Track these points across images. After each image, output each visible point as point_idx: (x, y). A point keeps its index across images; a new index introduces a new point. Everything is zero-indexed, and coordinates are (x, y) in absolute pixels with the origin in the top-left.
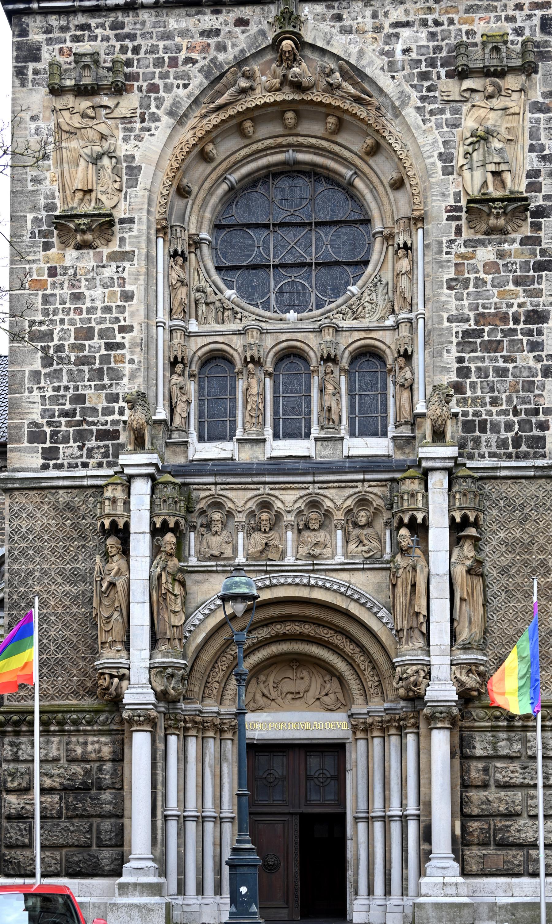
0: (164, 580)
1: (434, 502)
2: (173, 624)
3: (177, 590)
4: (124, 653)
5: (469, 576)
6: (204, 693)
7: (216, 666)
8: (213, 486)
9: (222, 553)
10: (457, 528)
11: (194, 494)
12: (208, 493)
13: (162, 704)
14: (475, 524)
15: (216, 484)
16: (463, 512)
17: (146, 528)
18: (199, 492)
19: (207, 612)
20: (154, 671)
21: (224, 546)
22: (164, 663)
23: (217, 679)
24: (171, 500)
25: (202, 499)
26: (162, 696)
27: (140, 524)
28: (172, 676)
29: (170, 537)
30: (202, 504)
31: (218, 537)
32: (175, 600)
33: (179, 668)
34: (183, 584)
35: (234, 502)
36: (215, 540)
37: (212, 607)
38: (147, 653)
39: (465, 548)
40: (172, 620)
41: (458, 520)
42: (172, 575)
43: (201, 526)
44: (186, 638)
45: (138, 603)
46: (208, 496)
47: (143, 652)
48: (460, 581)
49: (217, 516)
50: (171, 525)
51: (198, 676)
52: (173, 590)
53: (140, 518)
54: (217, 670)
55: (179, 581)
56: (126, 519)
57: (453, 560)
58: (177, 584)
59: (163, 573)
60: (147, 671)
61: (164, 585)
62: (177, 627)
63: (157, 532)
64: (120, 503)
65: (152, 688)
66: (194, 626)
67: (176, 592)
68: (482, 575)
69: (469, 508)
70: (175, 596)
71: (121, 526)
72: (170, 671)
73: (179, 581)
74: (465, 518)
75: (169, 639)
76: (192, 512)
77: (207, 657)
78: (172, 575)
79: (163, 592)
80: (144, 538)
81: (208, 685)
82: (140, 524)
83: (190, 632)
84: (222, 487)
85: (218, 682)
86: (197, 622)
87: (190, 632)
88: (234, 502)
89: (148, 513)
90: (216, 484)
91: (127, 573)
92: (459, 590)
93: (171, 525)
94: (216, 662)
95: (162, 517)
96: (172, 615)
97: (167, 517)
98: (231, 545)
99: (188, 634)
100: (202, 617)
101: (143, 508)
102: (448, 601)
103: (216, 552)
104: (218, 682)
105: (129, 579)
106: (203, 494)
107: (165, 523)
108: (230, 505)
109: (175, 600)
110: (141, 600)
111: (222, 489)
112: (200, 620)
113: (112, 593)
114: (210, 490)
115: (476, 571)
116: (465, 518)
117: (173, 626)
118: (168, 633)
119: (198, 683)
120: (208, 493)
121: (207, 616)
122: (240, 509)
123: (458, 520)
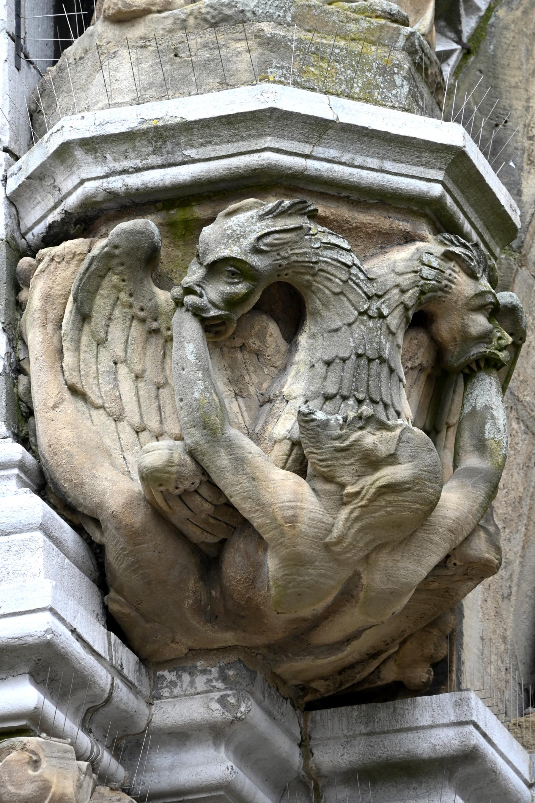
13: (191, 701)
22: (162, 138)
65: (43, 484)
72: (237, 230)
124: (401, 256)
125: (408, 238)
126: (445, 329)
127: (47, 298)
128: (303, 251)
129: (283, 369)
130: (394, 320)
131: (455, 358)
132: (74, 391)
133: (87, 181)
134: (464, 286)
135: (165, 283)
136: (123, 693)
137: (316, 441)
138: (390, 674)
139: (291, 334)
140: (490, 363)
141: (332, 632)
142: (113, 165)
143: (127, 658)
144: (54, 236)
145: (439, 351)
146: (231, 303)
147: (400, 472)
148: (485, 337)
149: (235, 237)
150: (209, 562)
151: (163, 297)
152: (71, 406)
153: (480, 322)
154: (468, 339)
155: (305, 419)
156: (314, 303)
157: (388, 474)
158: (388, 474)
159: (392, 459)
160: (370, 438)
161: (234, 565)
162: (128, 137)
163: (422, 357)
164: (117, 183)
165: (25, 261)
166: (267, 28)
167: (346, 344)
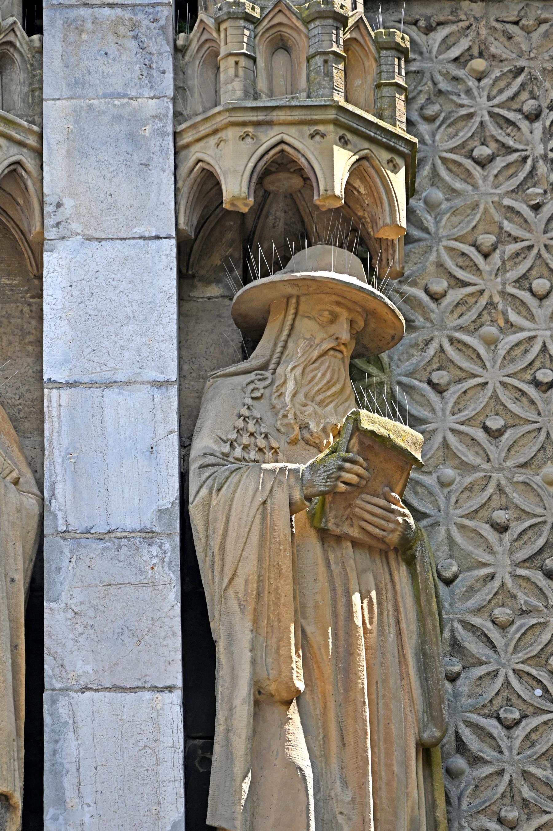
1: (77, 86)
5: (313, 546)
10: (227, 246)
14: (355, 231)
16: (269, 138)
39: (289, 375)
41: (235, 188)
48: (248, 569)
57: (203, 442)
68: (405, 550)
69: (310, 118)
74: (279, 171)
92: (244, 637)
102: (172, 706)
115: (359, 512)
116: (279, 171)
123: (235, 188)
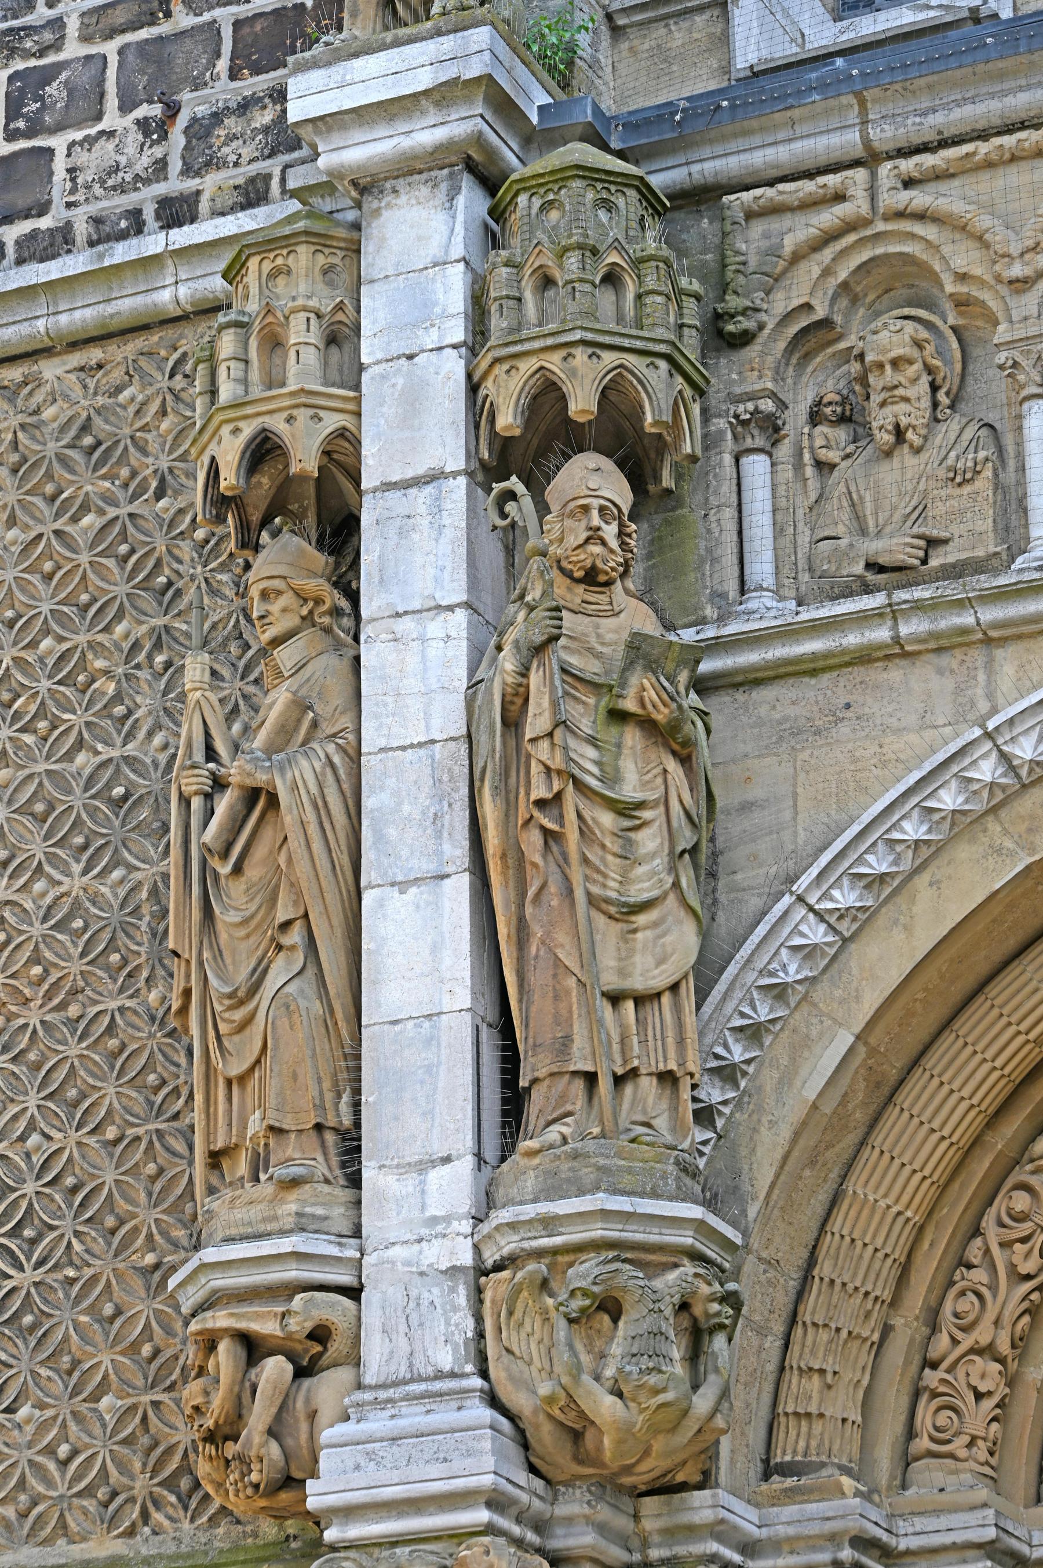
0: (538, 720)
2: (611, 981)
3: (638, 770)
4: (327, 1201)
6: (911, 1433)
7: (974, 1252)
8: (860, 175)
9: (932, 543)
11: (751, 242)
12: (828, 217)
13: (573, 1504)
15: (869, 159)
17: (447, 446)
18: (776, 224)
19: (845, 897)
20: (496, 1286)
21: (946, 502)
22: (549, 1223)
23: (982, 1335)
24: (573, 260)
25: (796, 258)
26: (550, 1446)
27: (414, 430)
28: (611, 1307)
29: (591, 479)
30: (805, 288)
31: (911, 461)
32: (624, 835)
33: (651, 1258)
34: (670, 737)
35: (981, 240)
36: (896, 481)
37: (878, 864)
38: (454, 1186)
40: (608, 959)
42: (595, 687)
43: (815, 418)
44: (727, 1073)
45: (403, 886)
46: (829, 237)
47: (437, 1176)
49: (890, 337)
50: (582, 403)
51: (848, 1314)
52: (612, 778)
53: (413, 401)
54: (979, 1276)
55: (647, 724)
56: (332, 422)
58: (632, 737)
59: (535, 679)
60: (462, 1297)
61: (542, 751)
62: (640, 1000)
63: (514, 459)
64: (302, 335)
65: (493, 1401)
66: (779, 992)
67: (630, 790)
70: (625, 809)
71: (305, 459)
72: (585, 1272)
73: (647, 724)
75: (591, 1078)
76: (745, 339)
77: (889, 1188)
78: (595, 687)
79: (540, 791)
80: (437, 508)
81: (932, 1378)
82: (414, 430)
83: (752, 1033)
84: (907, 166)
85: (987, 1351)
86: (793, 971)
87: (752, 1033)
88: (981, 240)
89: (455, 366)
90: (869, 159)
91: (346, 721)
93: (582, 403)
94: (976, 1232)
95: (527, 366)
96: (607, 931)
97: (554, 362)
98: (983, 483)
99: (738, 1053)
100: (816, 934)
101: (431, 340)
103: (897, 547)
104: (987, 1351)
105: (355, 757)
106: (798, 231)
107: (547, 395)
108: (963, 257)
109: (624, 835)
110: (427, 866)
111: (909, 183)
112: (808, 953)
113: (260, 851)
114: (840, 197)
117: (615, 999)
118: (580, 1042)
119: (854, 1367)
120: (828, 217)
121: (851, 929)
122: (1017, 271)
124: (672, 1276)
125: (676, 1266)
126: (697, 1310)
127: (493, 1302)
128: (620, 1280)
129: (612, 1339)
130: (668, 1311)
131: (704, 1325)
132: (509, 1351)
133: (509, 1244)
134: (705, 1289)
135: (551, 1295)
136: (537, 1503)
137: (626, 1381)
138: (680, 1478)
139: (615, 1320)
140: (722, 1327)
141: (643, 1467)
142: (522, 1235)
143: (538, 1484)
144: (498, 1268)
145: (695, 1320)
146: (583, 1310)
147: (669, 1396)
148: (718, 1314)
149: (584, 1277)
150: (577, 1436)
151: (550, 1302)
152: (506, 1358)
153: (715, 1307)
154: (708, 1316)
155: (620, 1370)
156: (626, 1306)
157: (662, 1398)
158: (662, 1398)
159: (664, 1390)
160: (652, 1380)
161: (589, 1436)
162: (530, 1221)
163: (686, 1323)
164: (526, 1245)
165: (483, 1279)
166: (602, 1161)
167: (645, 1326)
